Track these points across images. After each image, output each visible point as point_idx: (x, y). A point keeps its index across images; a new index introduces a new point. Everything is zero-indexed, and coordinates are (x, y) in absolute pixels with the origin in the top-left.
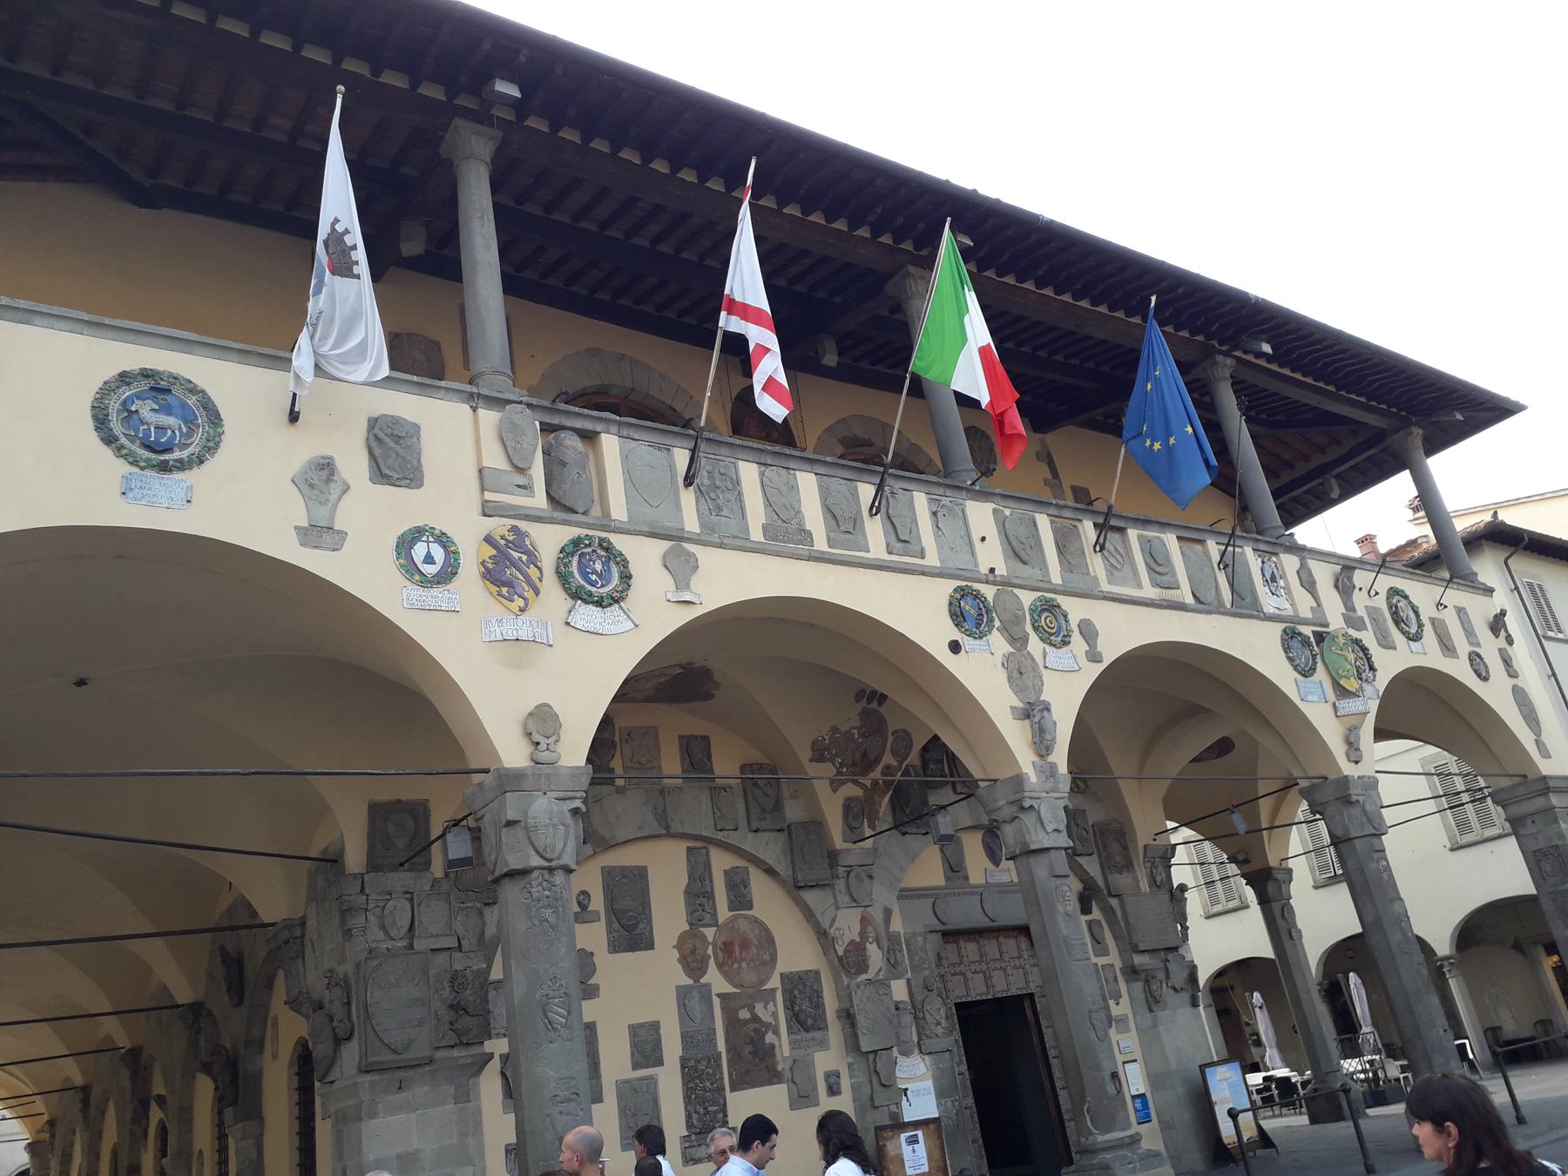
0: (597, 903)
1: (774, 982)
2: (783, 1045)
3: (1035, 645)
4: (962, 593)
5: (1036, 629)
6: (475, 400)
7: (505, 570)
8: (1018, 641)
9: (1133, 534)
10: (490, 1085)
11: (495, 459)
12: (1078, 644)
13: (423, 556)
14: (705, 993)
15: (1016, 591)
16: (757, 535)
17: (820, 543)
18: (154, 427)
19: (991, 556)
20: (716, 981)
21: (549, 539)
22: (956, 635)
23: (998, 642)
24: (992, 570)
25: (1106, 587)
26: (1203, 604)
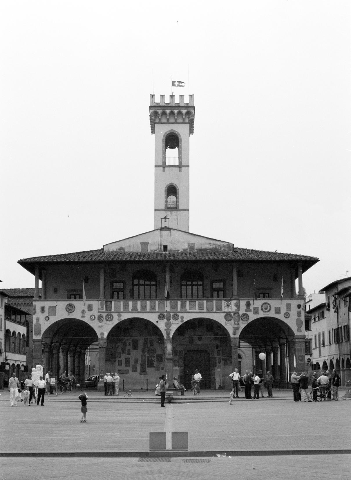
0: (131, 344)
1: (155, 355)
2: (155, 364)
4: (161, 314)
6: (98, 301)
7: (100, 319)
8: (169, 320)
9: (197, 302)
10: (117, 363)
11: (100, 307)
12: (180, 319)
13: (92, 318)
14: (145, 356)
16: (130, 310)
17: (139, 310)
18: (70, 308)
19: (168, 308)
20: (147, 355)
21: (104, 315)
22: (158, 320)
23: (165, 320)
25: (188, 311)
26: (209, 311)
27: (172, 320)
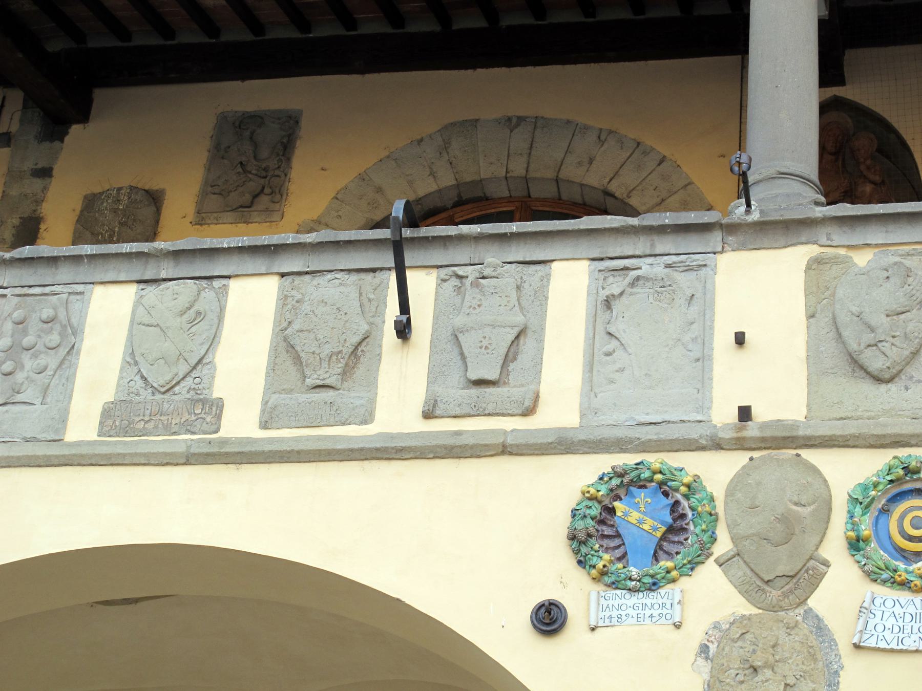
3: (841, 591)
4: (626, 483)
5: (856, 544)
15: (808, 455)
16: (82, 428)
22: (576, 591)
24: (745, 413)
27: (841, 591)
